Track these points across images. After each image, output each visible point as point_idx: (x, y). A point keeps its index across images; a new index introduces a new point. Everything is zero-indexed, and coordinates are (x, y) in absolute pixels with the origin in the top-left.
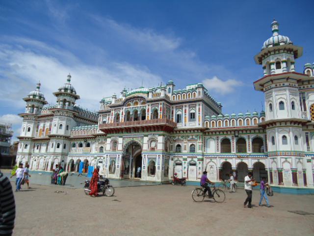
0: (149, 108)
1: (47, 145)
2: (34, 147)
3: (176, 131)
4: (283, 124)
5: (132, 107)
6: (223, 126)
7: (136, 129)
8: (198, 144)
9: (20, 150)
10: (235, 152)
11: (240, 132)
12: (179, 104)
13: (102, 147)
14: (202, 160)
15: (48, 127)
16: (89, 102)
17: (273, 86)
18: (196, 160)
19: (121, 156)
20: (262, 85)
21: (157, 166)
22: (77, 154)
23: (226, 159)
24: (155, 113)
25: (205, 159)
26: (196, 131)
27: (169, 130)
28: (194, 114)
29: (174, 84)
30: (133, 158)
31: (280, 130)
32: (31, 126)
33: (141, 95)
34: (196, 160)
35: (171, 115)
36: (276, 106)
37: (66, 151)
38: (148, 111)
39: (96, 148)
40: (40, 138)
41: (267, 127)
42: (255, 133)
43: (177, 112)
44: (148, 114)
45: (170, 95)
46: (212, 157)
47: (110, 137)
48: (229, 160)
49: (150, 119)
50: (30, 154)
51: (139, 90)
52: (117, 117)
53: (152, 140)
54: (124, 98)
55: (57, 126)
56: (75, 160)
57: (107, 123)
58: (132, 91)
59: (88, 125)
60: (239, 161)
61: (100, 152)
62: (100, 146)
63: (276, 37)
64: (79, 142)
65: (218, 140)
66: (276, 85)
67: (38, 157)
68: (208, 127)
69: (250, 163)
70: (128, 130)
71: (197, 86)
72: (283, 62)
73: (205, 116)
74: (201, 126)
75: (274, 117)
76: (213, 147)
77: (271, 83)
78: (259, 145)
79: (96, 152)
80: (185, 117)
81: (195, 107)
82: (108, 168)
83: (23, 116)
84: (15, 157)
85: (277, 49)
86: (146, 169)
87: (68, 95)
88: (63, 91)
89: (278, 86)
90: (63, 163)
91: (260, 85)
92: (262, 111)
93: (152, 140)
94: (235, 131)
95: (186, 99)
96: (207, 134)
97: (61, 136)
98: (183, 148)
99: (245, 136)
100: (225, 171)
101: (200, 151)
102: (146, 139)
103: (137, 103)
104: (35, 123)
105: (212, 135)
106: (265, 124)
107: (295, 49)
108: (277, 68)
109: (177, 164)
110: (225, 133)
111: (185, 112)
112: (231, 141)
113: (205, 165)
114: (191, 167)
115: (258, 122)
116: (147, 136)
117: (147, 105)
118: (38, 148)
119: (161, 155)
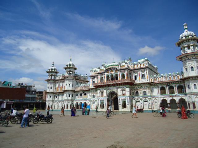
0: (120, 74)
1: (62, 96)
2: (55, 97)
3: (135, 85)
4: (194, 78)
6: (161, 80)
7: (113, 85)
8: (148, 90)
9: (47, 99)
10: (168, 94)
11: (170, 83)
12: (136, 70)
13: (94, 95)
14: (151, 99)
15: (62, 86)
16: (82, 71)
17: (187, 59)
18: (147, 99)
19: (106, 99)
20: (181, 58)
21: (127, 103)
22: (80, 99)
24: (123, 76)
25: (152, 98)
26: (146, 84)
27: (131, 84)
28: (144, 75)
29: (131, 59)
30: (113, 100)
31: (192, 81)
32: (52, 86)
33: (114, 67)
34: (147, 99)
35: (131, 76)
36: (189, 69)
37: (73, 98)
38: (119, 75)
39: (90, 95)
40: (57, 92)
41: (185, 80)
42: (178, 83)
43: (134, 74)
45: (130, 65)
46: (155, 97)
47: (99, 90)
48: (165, 98)
49: (120, 79)
50: (53, 101)
51: (112, 64)
52: (102, 78)
53: (123, 90)
54: (105, 69)
55: (67, 85)
56: (79, 102)
57: (95, 82)
58: (109, 64)
59: (84, 83)
60: (171, 98)
61: (93, 97)
62: (93, 95)
63: (186, 33)
64: (80, 93)
65: (158, 88)
67: (58, 102)
68: (153, 81)
69: (177, 99)
70: (109, 86)
71: (144, 60)
72: (191, 46)
73: (150, 75)
74: (148, 81)
76: (156, 91)
77: (185, 57)
78: (181, 89)
79: (91, 98)
80: (139, 77)
81: (144, 71)
83: (47, 81)
84: (45, 103)
85: (187, 40)
86: (121, 105)
87: (71, 68)
88: (69, 66)
89: (189, 59)
90: (72, 105)
91: (180, 58)
92: (182, 72)
93: (123, 90)
94: (168, 83)
95: (139, 67)
96: (152, 85)
97: (70, 90)
98: (139, 93)
99: (173, 85)
100: (164, 104)
101: (149, 95)
102: (119, 90)
103: (112, 71)
104: (54, 84)
105: (155, 85)
106: (183, 79)
107: (197, 39)
108: (188, 49)
109: (137, 102)
110: (162, 84)
111: (139, 74)
112: (166, 88)
113: (152, 102)
115: (180, 78)
117: (118, 72)
119: (129, 98)
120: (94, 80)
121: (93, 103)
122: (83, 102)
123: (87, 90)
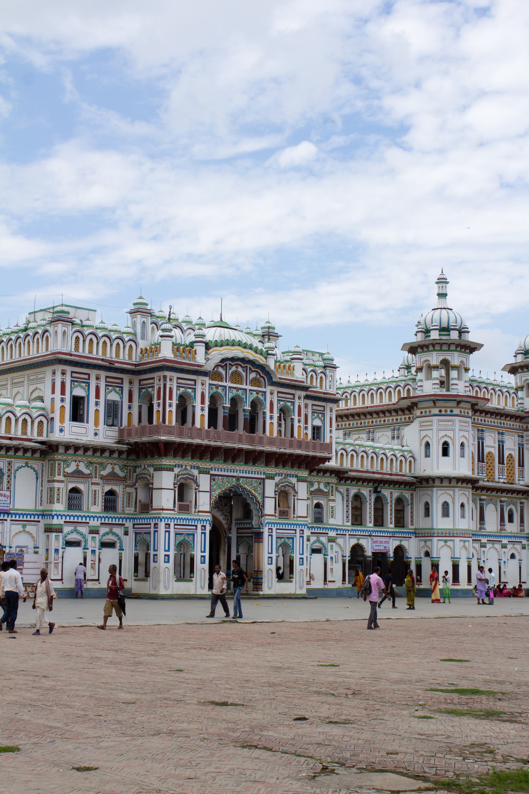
5: (228, 388)
13: (75, 490)
17: (456, 411)
18: (323, 539)
19: (208, 528)
23: (358, 539)
34: (323, 539)
38: (271, 411)
44: (271, 418)
62: (71, 486)
66: (461, 412)
70: (231, 455)
75: (454, 469)
82: (171, 565)
94: (378, 484)
99: (386, 492)
103: (236, 377)
111: (306, 422)
114: (315, 555)
116: (273, 478)
117: (269, 389)
120: (79, 392)
121: (69, 544)
123: (26, 450)
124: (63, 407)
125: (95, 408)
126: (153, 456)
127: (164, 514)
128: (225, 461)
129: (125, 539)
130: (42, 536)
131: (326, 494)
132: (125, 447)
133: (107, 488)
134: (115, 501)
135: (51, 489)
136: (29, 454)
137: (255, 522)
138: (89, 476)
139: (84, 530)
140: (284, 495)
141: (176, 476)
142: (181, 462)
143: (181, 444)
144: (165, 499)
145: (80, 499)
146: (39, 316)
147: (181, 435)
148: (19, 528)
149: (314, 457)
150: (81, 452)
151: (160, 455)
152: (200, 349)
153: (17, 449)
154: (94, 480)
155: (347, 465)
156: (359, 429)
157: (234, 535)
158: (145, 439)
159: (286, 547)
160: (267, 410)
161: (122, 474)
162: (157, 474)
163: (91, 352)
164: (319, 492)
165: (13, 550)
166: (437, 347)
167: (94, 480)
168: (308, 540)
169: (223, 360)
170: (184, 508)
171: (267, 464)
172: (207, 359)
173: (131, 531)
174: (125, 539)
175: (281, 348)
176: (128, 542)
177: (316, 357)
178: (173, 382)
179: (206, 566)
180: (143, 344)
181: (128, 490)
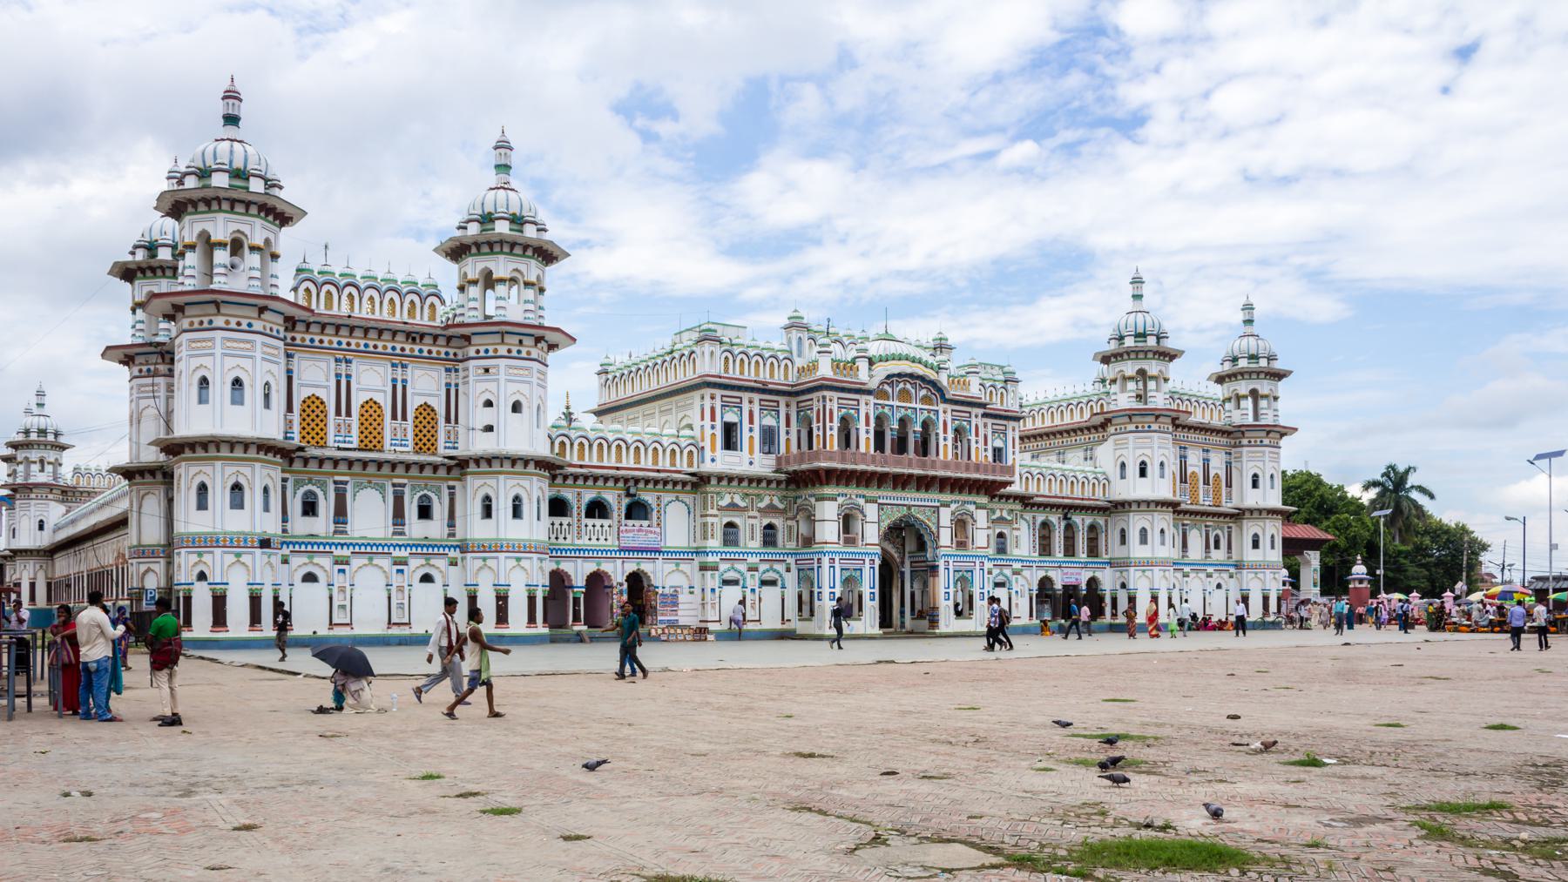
5: (896, 408)
13: (730, 525)
15: (385, 401)
18: (1007, 572)
19: (878, 562)
28: (1000, 450)
33: (919, 370)
34: (1007, 572)
38: (945, 431)
48: (1052, 574)
51: (893, 348)
61: (726, 543)
64: (589, 495)
70: (901, 482)
94: (1067, 509)
99: (1077, 519)
117: (941, 407)
118: (310, 508)
120: (731, 417)
121: (726, 582)
122: (618, 572)
123: (675, 483)
124: (713, 435)
125: (749, 435)
126: (814, 485)
127: (828, 548)
128: (894, 488)
129: (787, 576)
130: (697, 574)
131: (1010, 522)
132: (783, 476)
133: (766, 522)
134: (775, 536)
135: (705, 525)
136: (679, 487)
137: (929, 555)
138: (745, 509)
139: (742, 567)
140: (961, 523)
141: (840, 506)
142: (845, 490)
143: (844, 471)
144: (828, 531)
145: (736, 534)
146: (685, 336)
147: (843, 460)
148: (672, 566)
149: (994, 482)
150: (735, 483)
151: (821, 484)
152: (863, 365)
153: (666, 483)
154: (751, 513)
155: (1032, 490)
156: (1047, 451)
157: (907, 569)
158: (804, 467)
159: (964, 581)
160: (941, 431)
161: (781, 506)
162: (818, 505)
163: (742, 373)
164: (1001, 520)
165: (667, 591)
166: (1133, 356)
167: (751, 513)
168: (990, 573)
169: (888, 377)
170: (850, 541)
171: (941, 491)
172: (871, 377)
173: (793, 567)
174: (787, 576)
175: (955, 363)
176: (791, 579)
177: (996, 371)
178: (833, 401)
179: (876, 603)
180: (799, 362)
181: (790, 523)
